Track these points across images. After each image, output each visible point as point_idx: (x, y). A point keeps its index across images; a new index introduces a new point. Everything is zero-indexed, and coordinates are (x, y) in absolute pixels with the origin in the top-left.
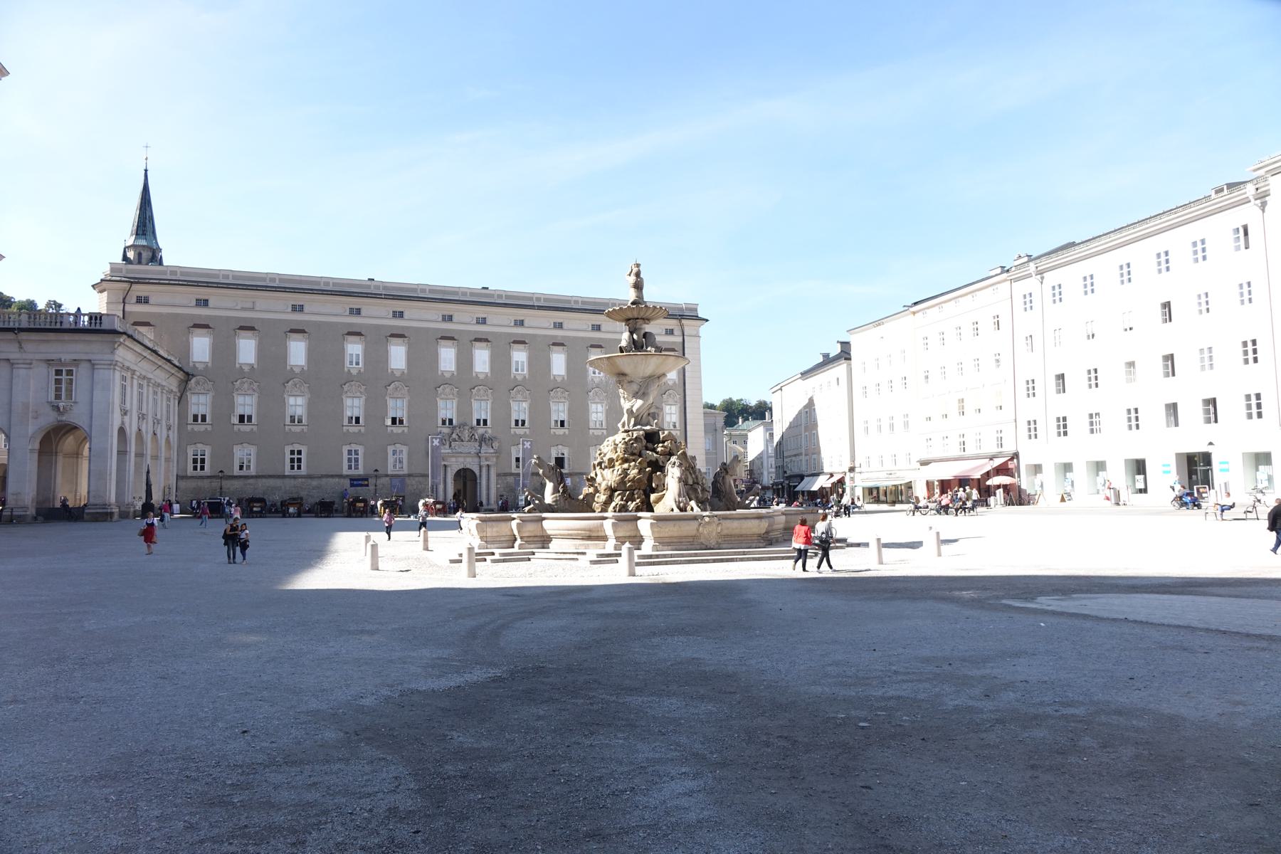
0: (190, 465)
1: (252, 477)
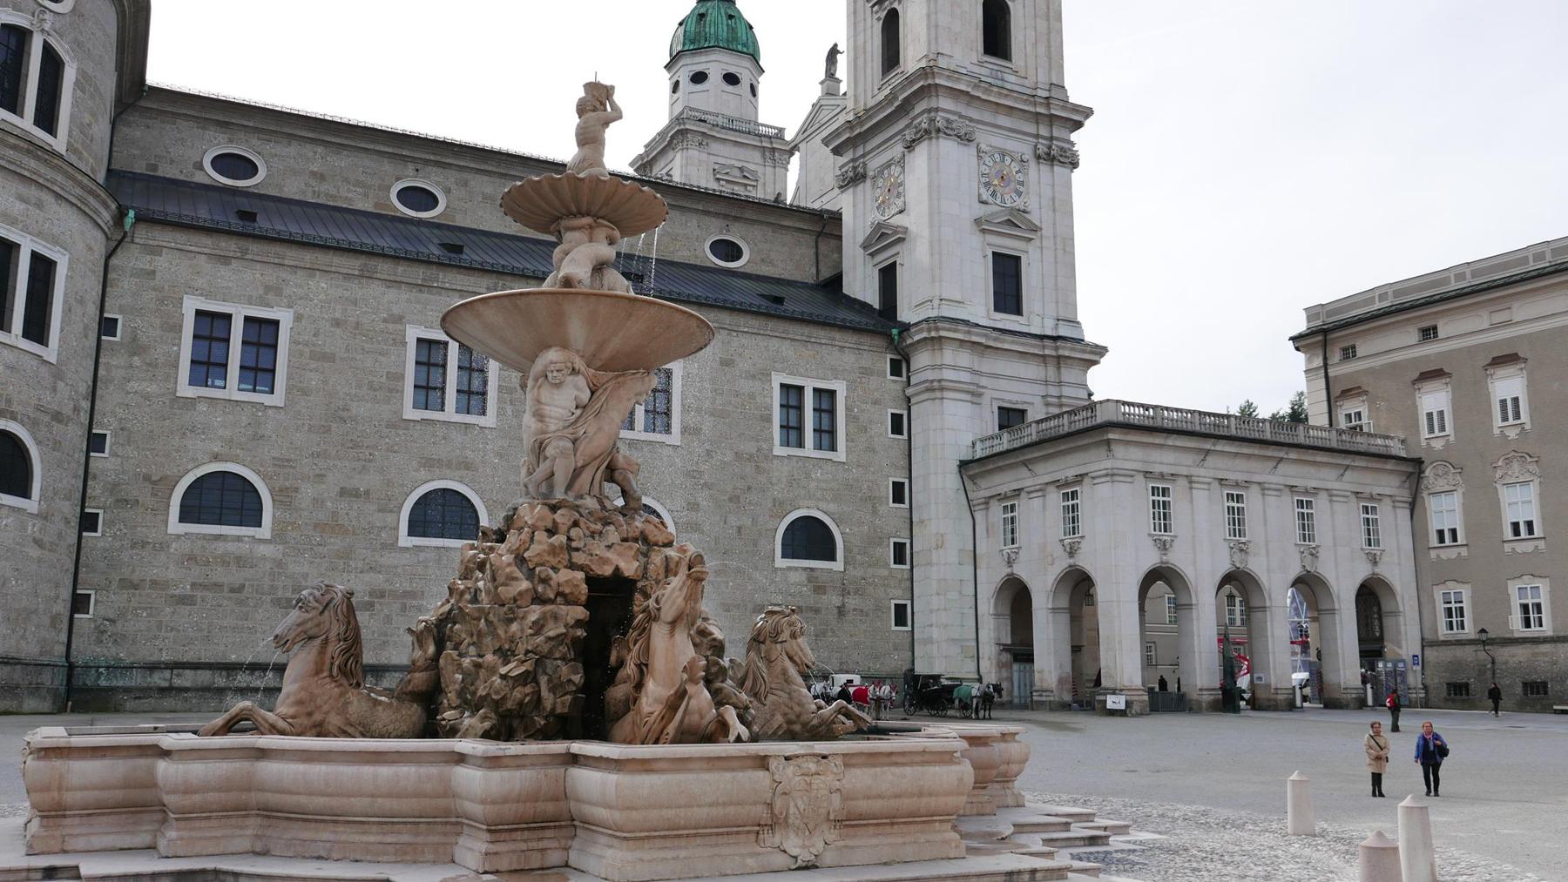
0: (1442, 620)
1: (1545, 640)
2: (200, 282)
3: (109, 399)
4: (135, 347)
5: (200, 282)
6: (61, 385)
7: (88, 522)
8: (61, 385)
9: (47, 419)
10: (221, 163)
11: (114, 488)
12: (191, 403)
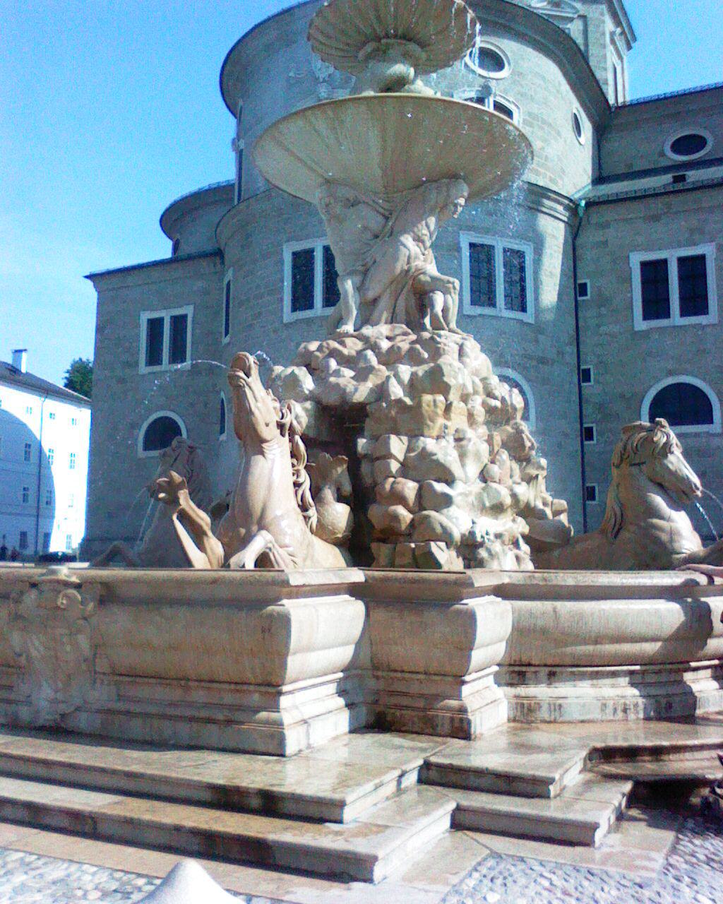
2: (640, 239)
3: (588, 341)
4: (602, 301)
5: (640, 239)
6: (541, 338)
7: (588, 434)
8: (541, 338)
9: (534, 363)
10: (679, 146)
11: (601, 407)
12: (646, 334)
